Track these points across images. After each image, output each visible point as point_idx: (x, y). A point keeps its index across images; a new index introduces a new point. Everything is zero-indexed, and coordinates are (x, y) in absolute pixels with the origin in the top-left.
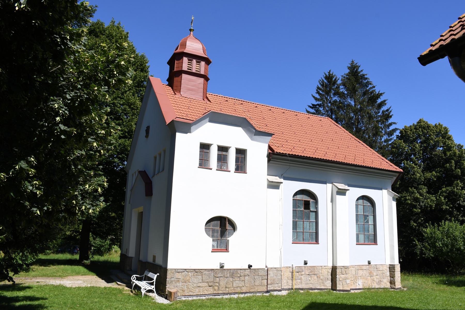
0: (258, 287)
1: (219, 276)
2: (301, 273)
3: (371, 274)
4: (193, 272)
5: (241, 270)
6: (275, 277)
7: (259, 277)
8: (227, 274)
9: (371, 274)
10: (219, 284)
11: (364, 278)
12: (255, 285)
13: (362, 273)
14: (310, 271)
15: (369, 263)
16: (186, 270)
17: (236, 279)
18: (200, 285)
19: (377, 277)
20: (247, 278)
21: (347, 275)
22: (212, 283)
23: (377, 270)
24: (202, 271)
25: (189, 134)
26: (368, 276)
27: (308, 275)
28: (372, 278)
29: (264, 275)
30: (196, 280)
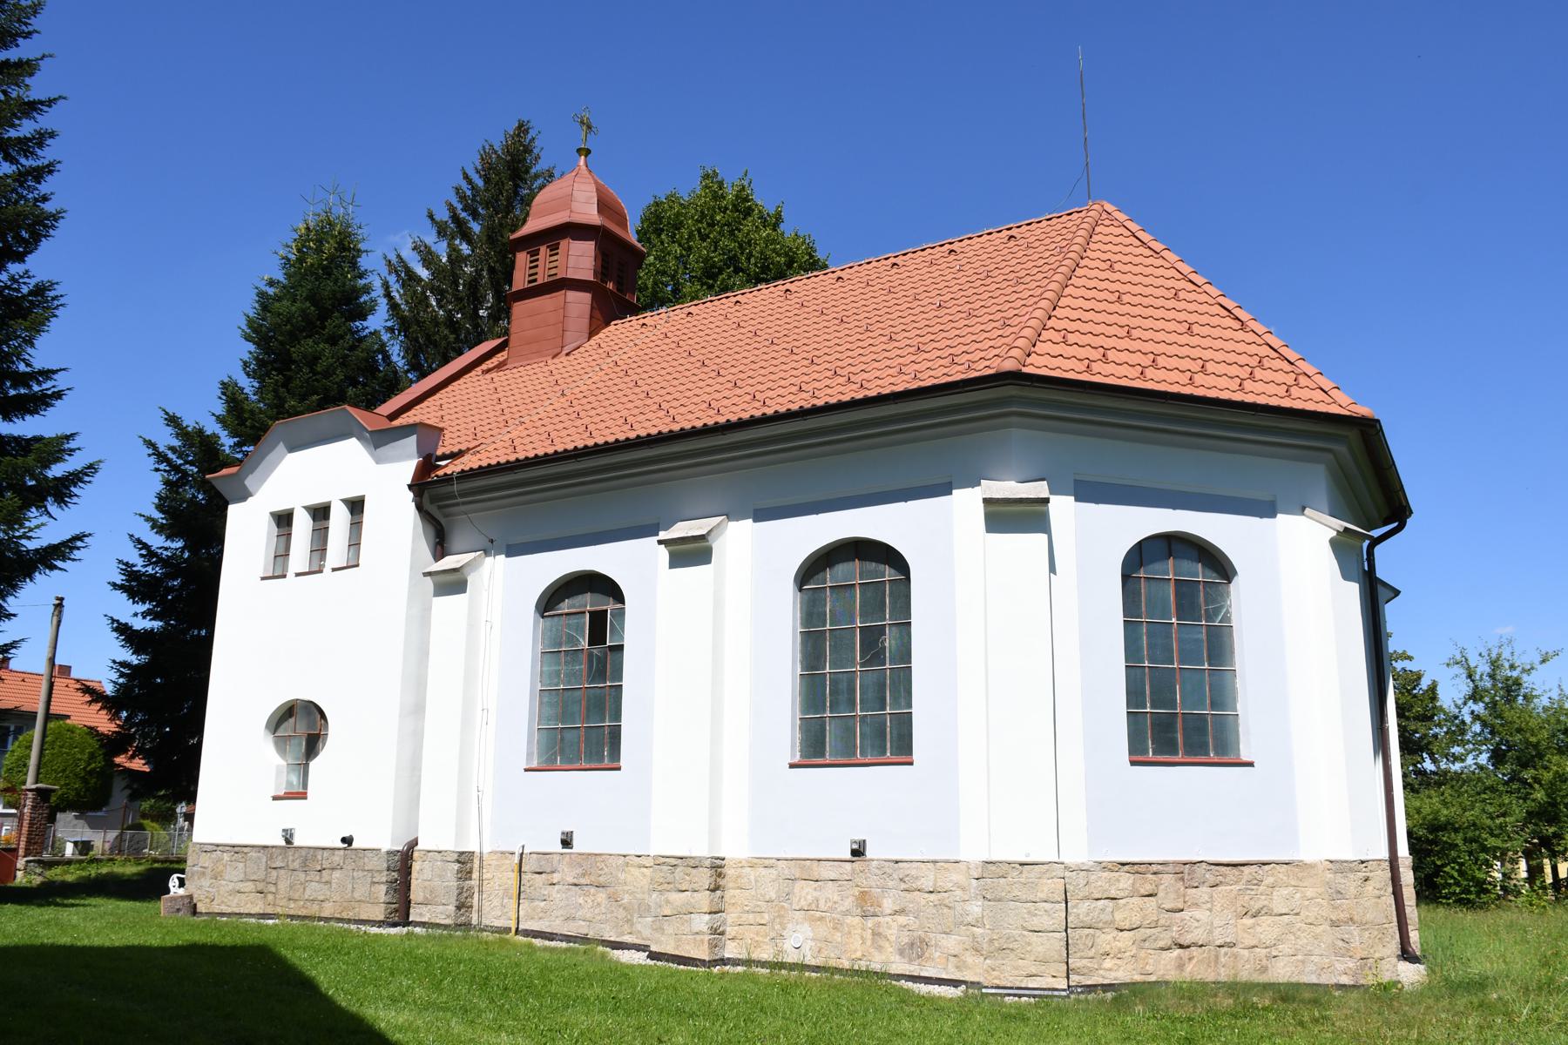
0: (363, 905)
1: (278, 864)
2: (550, 876)
3: (866, 906)
4: (231, 852)
5: (325, 852)
6: (437, 883)
7: (366, 873)
8: (293, 861)
9: (866, 906)
10: (277, 890)
11: (821, 919)
12: (354, 898)
13: (816, 894)
14: (579, 871)
15: (858, 852)
16: (218, 846)
17: (313, 876)
18: (241, 886)
19: (902, 919)
20: (337, 874)
21: (695, 894)
22: (262, 884)
23: (903, 886)
24: (245, 850)
25: (250, 499)
26: (847, 913)
27: (576, 885)
28: (870, 922)
29: (379, 868)
30: (234, 873)
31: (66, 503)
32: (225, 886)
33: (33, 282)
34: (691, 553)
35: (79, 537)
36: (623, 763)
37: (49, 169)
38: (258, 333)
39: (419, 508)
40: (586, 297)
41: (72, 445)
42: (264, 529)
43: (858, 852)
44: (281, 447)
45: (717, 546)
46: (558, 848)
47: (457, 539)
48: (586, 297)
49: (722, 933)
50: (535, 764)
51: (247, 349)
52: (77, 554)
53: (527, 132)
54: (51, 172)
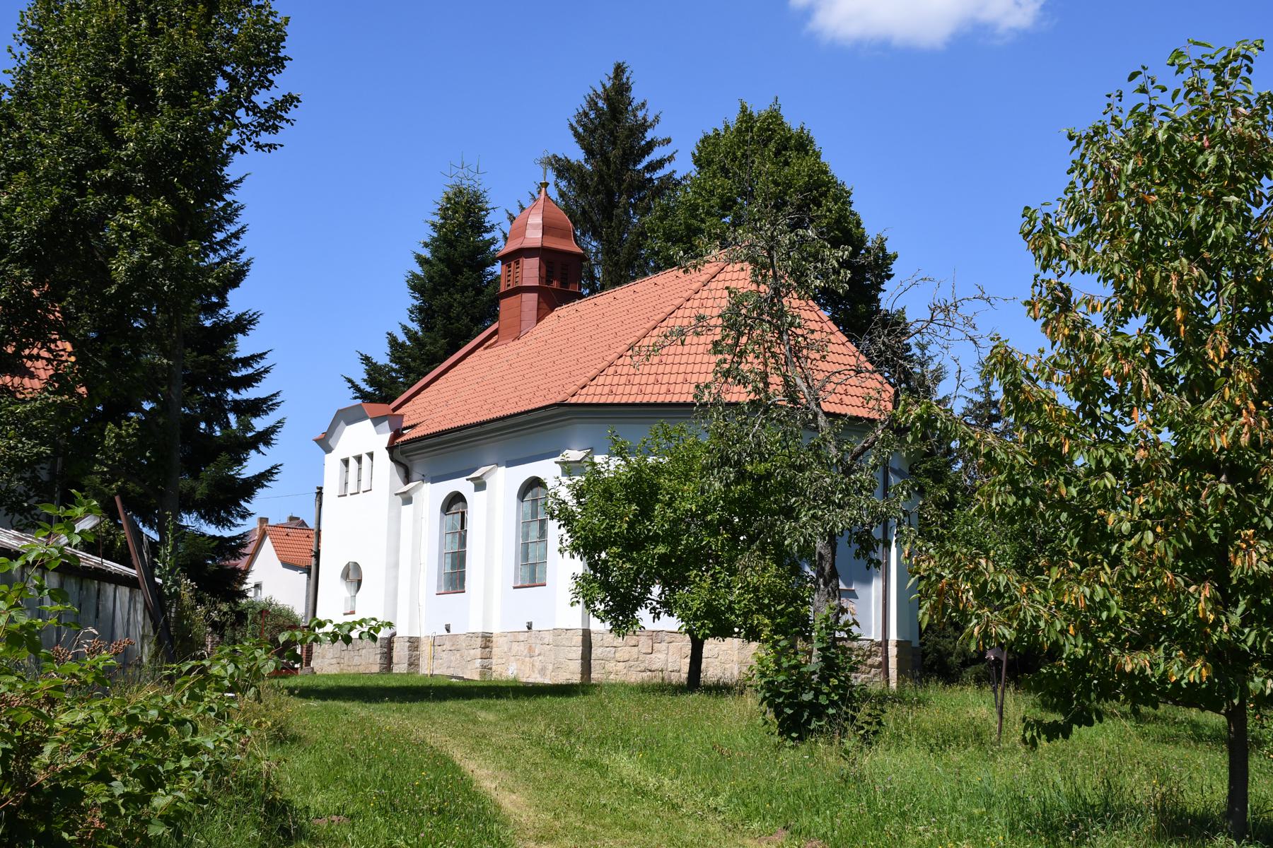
15: (529, 628)
17: (356, 653)
19: (540, 658)
20: (364, 651)
31: (271, 444)
32: (327, 661)
33: (234, 316)
34: (480, 485)
35: (275, 467)
36: (466, 589)
37: (242, 230)
38: (416, 285)
39: (392, 459)
40: (534, 296)
41: (278, 399)
42: (339, 465)
43: (529, 628)
44: (342, 423)
45: (488, 481)
46: (446, 633)
47: (415, 475)
48: (534, 296)
49: (491, 669)
50: (443, 591)
51: (408, 300)
52: (276, 477)
53: (623, 71)
54: (243, 232)
